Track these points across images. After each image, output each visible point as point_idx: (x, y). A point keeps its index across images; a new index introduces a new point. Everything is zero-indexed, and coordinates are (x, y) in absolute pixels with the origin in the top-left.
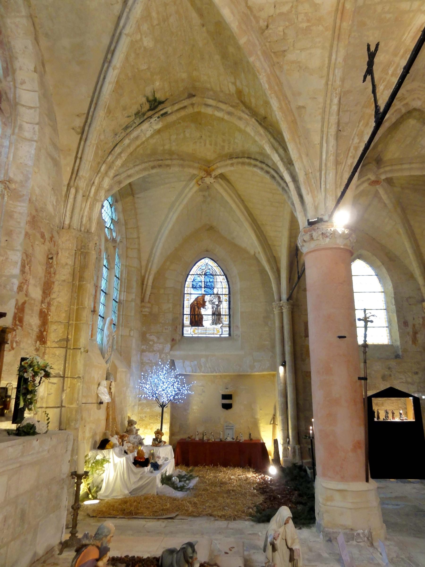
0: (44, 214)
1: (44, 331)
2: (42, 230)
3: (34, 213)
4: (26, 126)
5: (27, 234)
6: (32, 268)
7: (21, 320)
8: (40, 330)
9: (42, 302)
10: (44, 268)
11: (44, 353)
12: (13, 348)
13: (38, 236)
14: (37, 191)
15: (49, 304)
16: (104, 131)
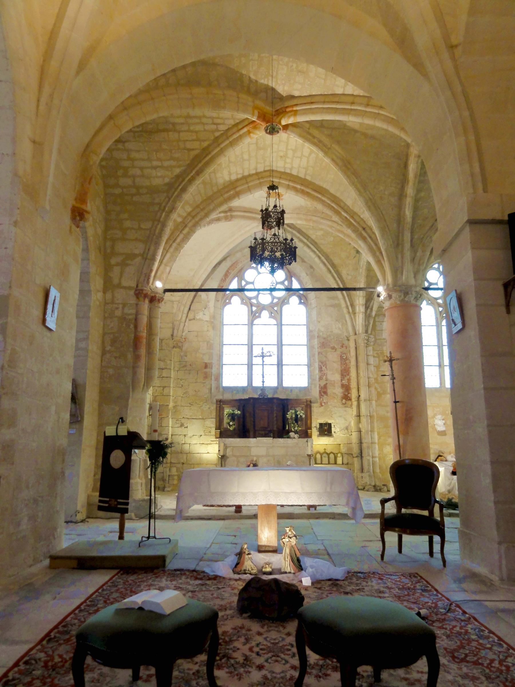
0: (332, 337)
1: (348, 394)
2: (331, 346)
3: (323, 340)
4: (313, 301)
5: (319, 353)
6: (328, 367)
7: (325, 393)
8: (344, 394)
9: (342, 380)
10: (339, 363)
11: (352, 405)
12: (322, 406)
13: (330, 350)
14: (322, 329)
15: (349, 380)
16: (348, 274)
